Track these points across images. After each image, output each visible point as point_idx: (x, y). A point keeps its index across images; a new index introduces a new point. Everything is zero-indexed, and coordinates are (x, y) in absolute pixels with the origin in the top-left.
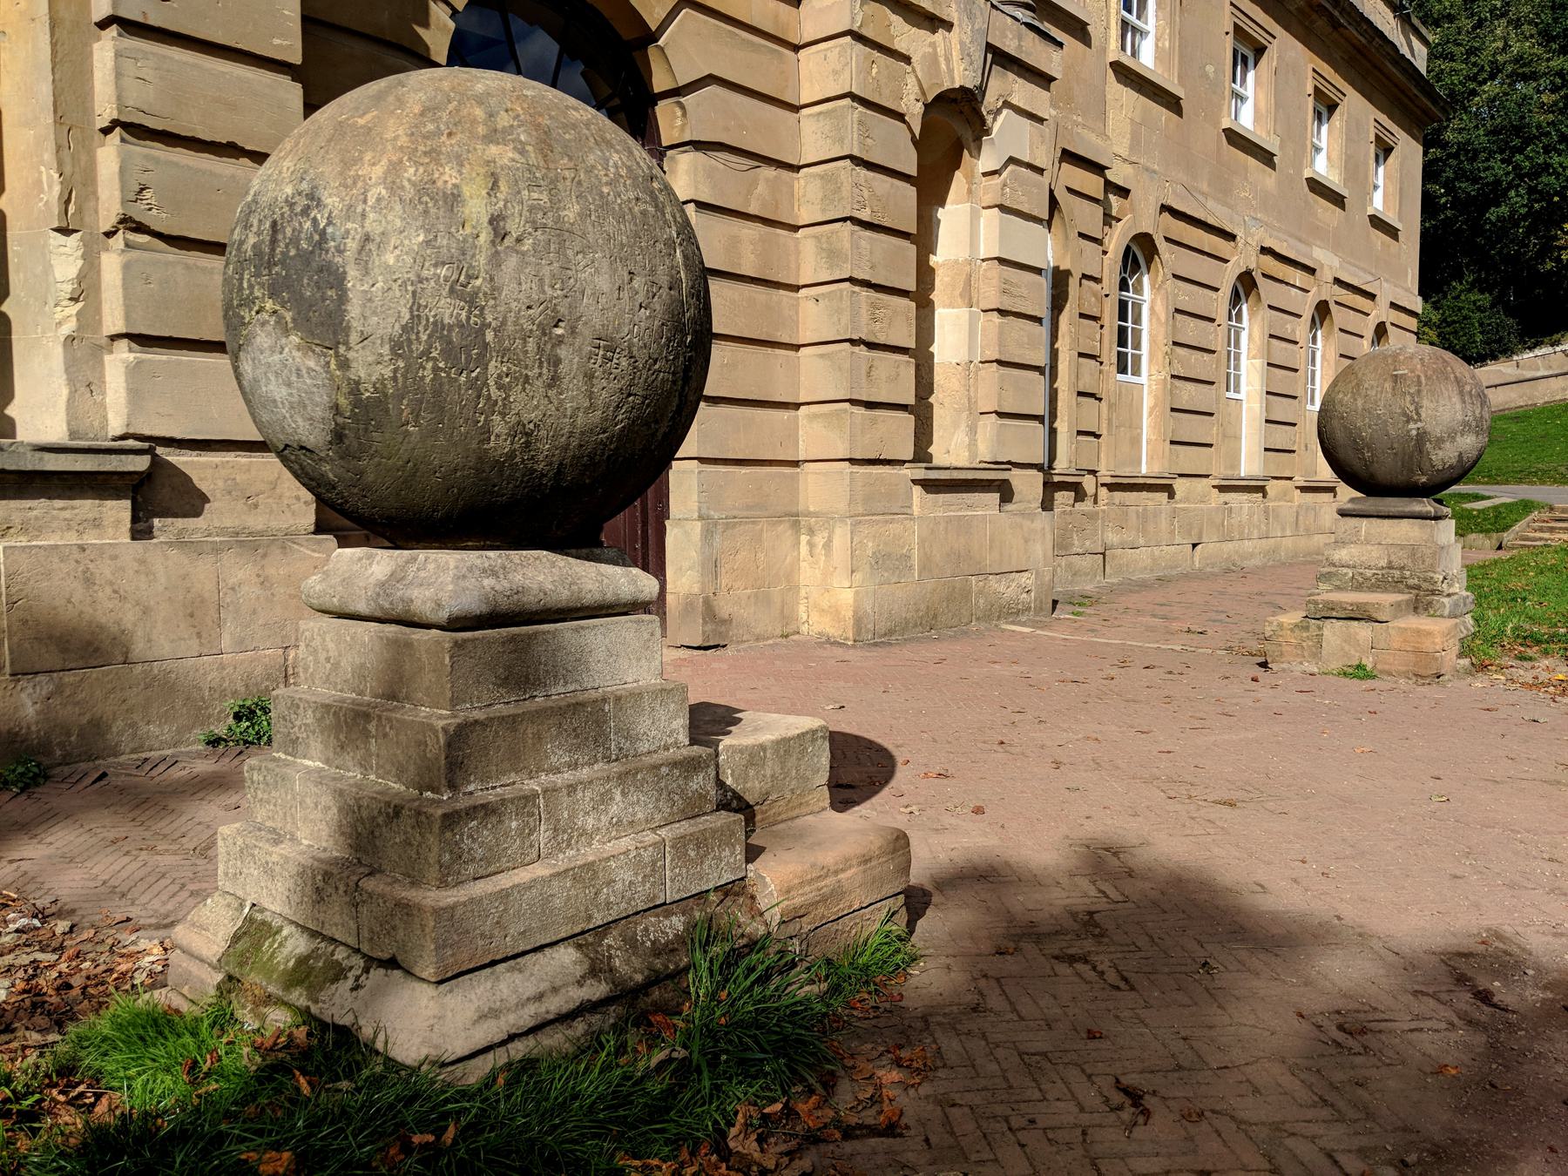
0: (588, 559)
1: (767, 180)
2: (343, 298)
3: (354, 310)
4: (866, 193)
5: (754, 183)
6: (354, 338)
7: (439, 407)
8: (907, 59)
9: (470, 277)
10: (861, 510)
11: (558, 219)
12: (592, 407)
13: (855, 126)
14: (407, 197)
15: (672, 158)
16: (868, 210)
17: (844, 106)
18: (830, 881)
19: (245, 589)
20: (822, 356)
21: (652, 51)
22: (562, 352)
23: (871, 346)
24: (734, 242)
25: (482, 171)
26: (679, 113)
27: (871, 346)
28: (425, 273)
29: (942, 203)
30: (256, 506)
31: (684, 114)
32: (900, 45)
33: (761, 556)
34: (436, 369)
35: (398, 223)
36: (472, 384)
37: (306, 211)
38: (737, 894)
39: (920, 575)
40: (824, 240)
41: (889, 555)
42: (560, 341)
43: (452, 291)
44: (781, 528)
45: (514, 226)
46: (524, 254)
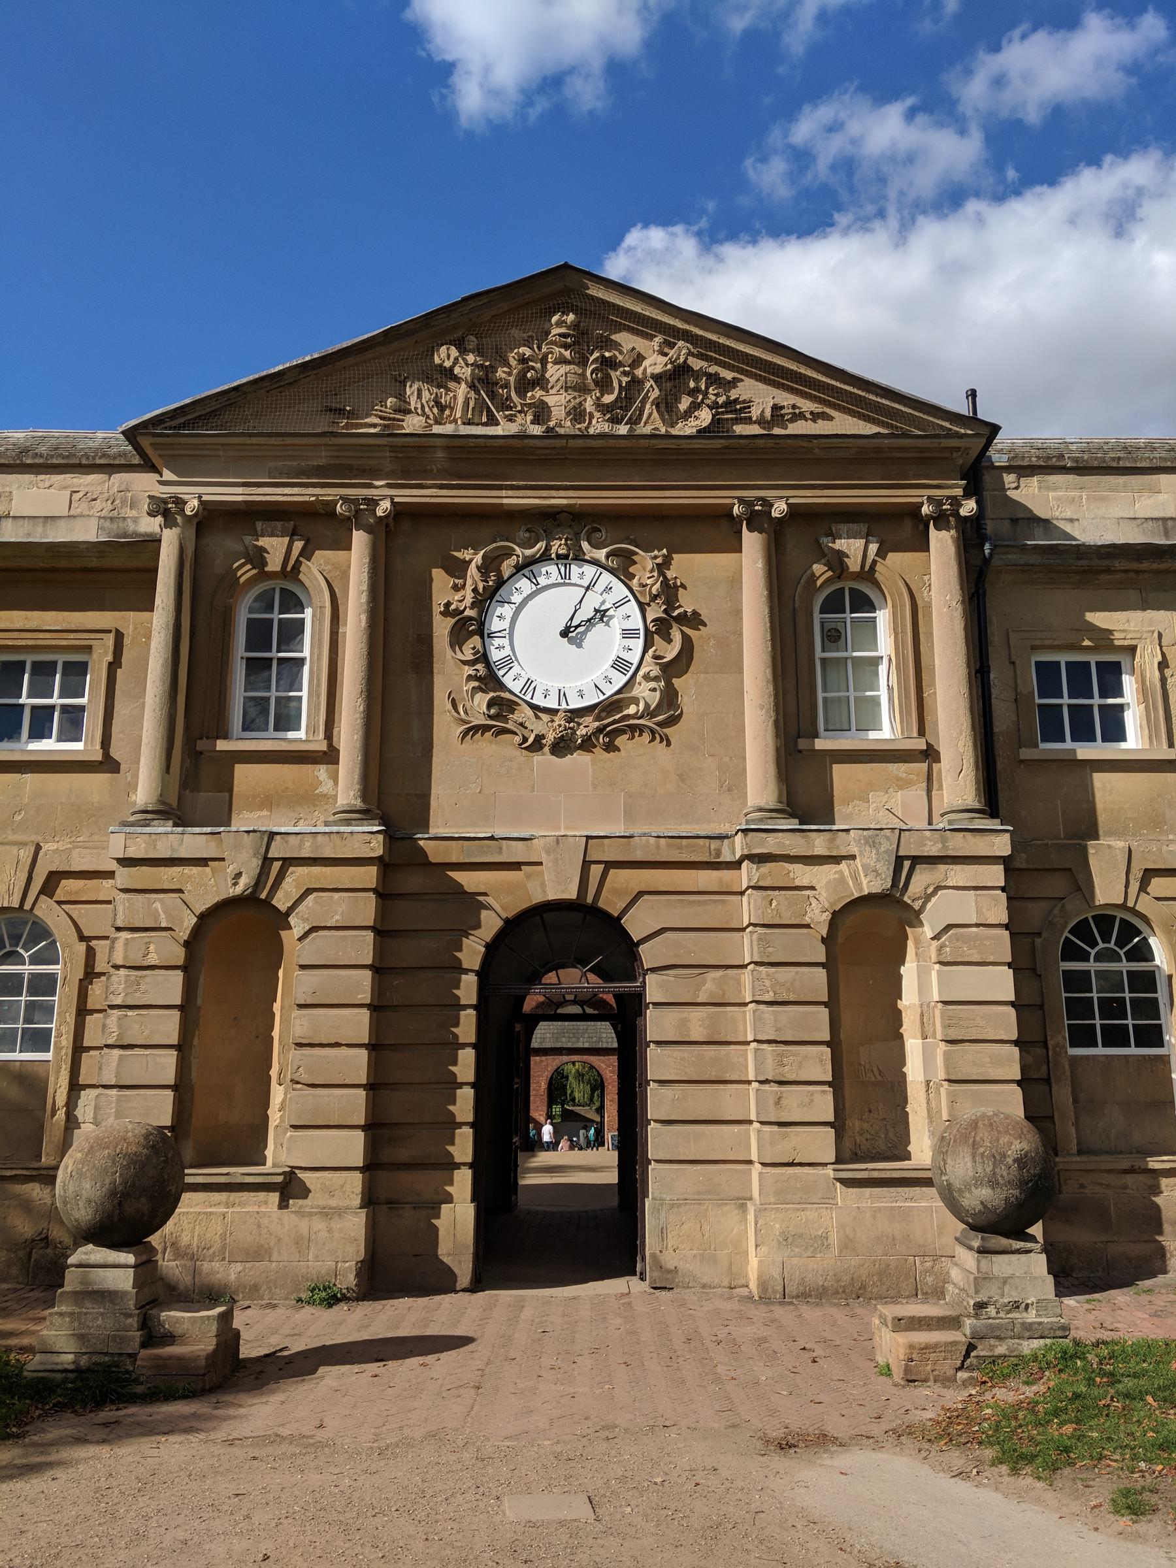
1: (714, 979)
4: (768, 983)
10: (772, 1200)
13: (755, 943)
16: (772, 994)
19: (321, 1233)
23: (781, 1083)
24: (684, 1022)
29: (903, 963)
30: (333, 1196)
33: (706, 1227)
39: (840, 1252)
41: (801, 1236)
44: (727, 1208)
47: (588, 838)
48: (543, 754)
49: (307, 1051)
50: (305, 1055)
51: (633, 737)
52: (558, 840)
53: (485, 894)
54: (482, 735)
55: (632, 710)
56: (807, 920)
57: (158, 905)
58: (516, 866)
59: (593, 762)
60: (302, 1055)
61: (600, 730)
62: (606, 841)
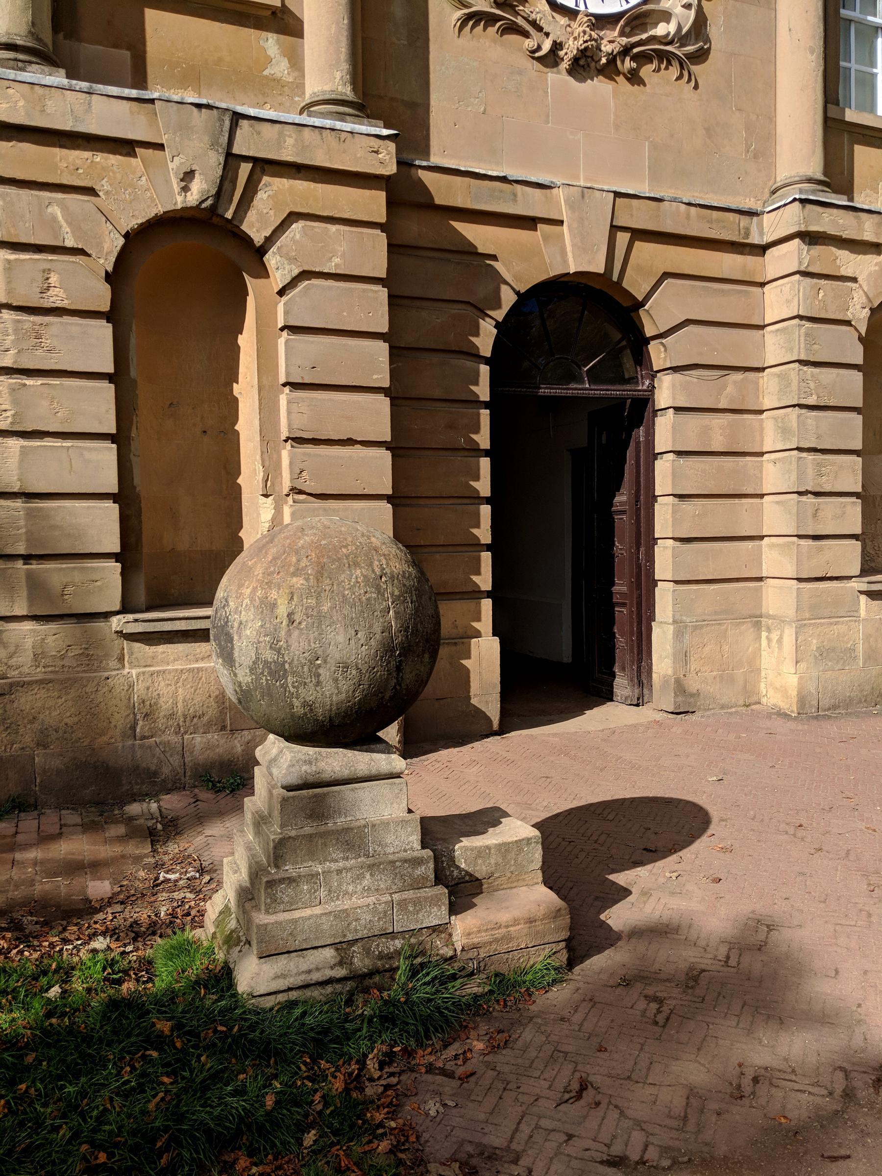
0: (366, 751)
1: (735, 382)
2: (232, 648)
3: (236, 654)
4: (812, 385)
5: (724, 387)
6: (237, 665)
7: (270, 695)
8: (854, 280)
9: (278, 641)
10: (807, 615)
11: (319, 612)
12: (339, 693)
13: (802, 339)
14: (256, 604)
15: (660, 379)
16: (815, 397)
17: (793, 325)
18: (503, 931)
20: (778, 503)
21: (641, 312)
22: (321, 671)
23: (817, 494)
24: (706, 431)
25: (287, 591)
26: (663, 350)
27: (817, 494)
28: (261, 639)
31: (666, 350)
32: (844, 272)
33: (726, 648)
34: (267, 680)
35: (252, 617)
36: (282, 686)
37: (224, 607)
38: (441, 932)
39: (864, 663)
40: (780, 420)
41: (833, 649)
42: (319, 666)
43: (271, 647)
44: (743, 627)
45: (297, 617)
46: (301, 629)
47: (617, 194)
48: (559, 73)
49: (310, 449)
50: (309, 455)
51: (659, 70)
52: (583, 192)
53: (494, 258)
54: (485, 29)
55: (661, 30)
56: (849, 316)
57: (56, 210)
58: (529, 222)
59: (615, 94)
60: (305, 454)
61: (626, 51)
62: (635, 202)
